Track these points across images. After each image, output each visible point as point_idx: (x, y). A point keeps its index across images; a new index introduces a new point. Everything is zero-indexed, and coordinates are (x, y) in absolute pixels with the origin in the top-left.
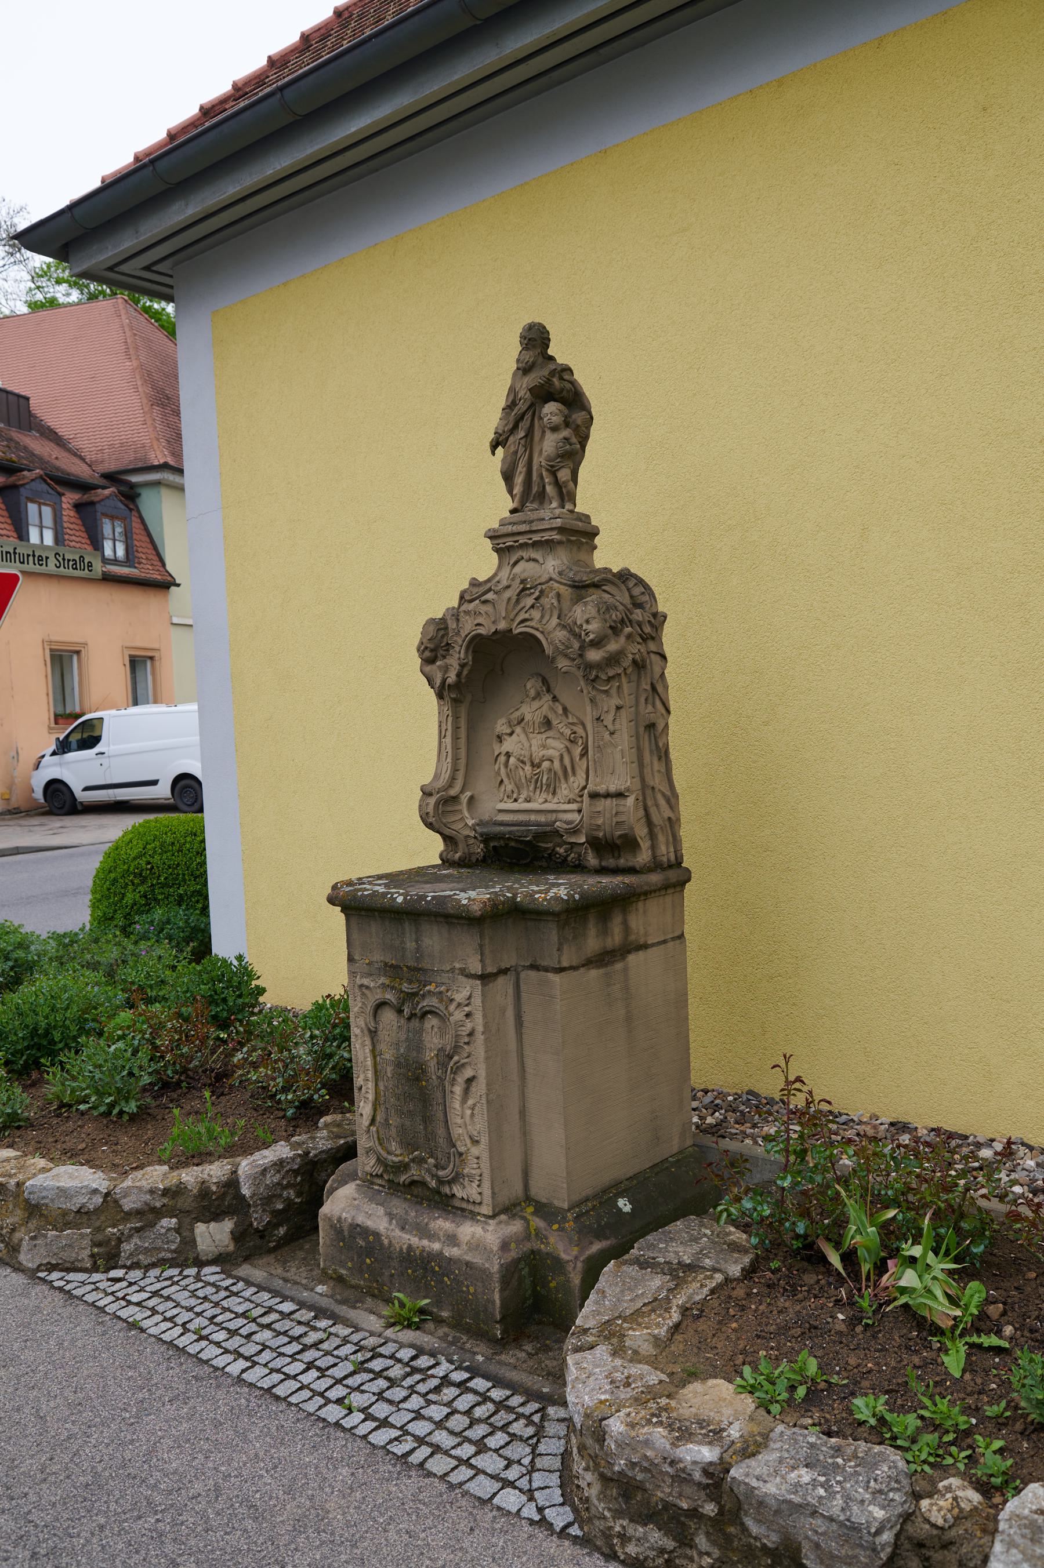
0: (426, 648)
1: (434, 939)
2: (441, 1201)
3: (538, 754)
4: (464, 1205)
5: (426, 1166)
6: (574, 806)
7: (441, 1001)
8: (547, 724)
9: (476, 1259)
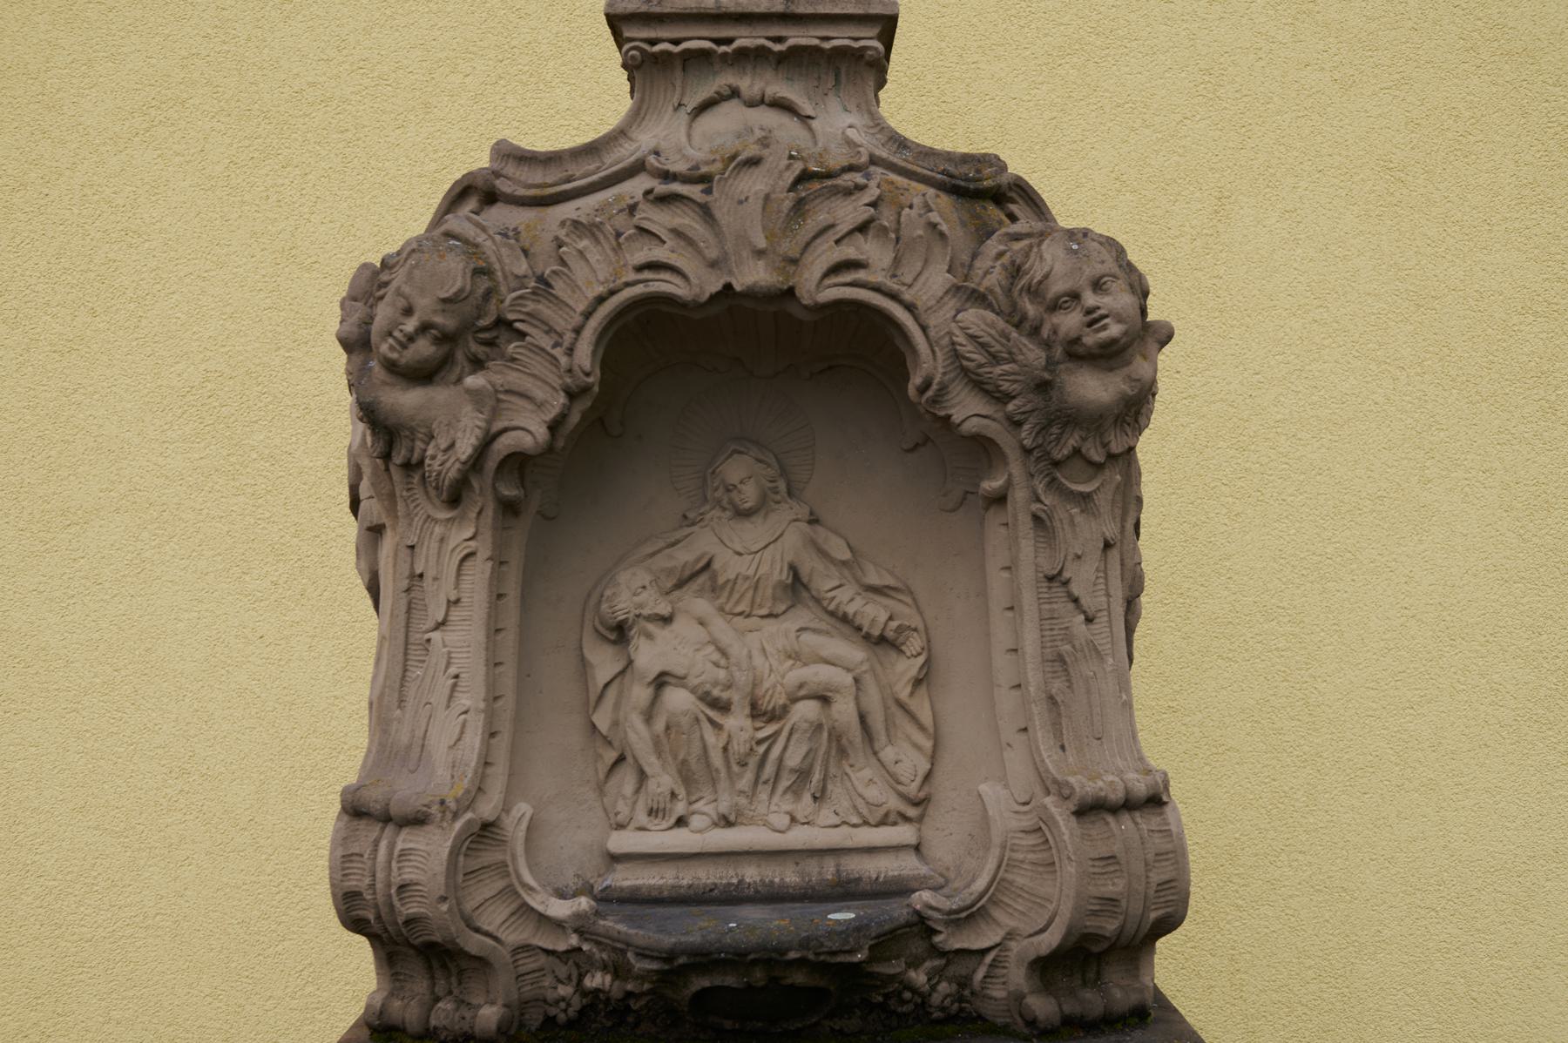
0: (424, 328)
3: (780, 678)
6: (903, 834)
8: (796, 586)
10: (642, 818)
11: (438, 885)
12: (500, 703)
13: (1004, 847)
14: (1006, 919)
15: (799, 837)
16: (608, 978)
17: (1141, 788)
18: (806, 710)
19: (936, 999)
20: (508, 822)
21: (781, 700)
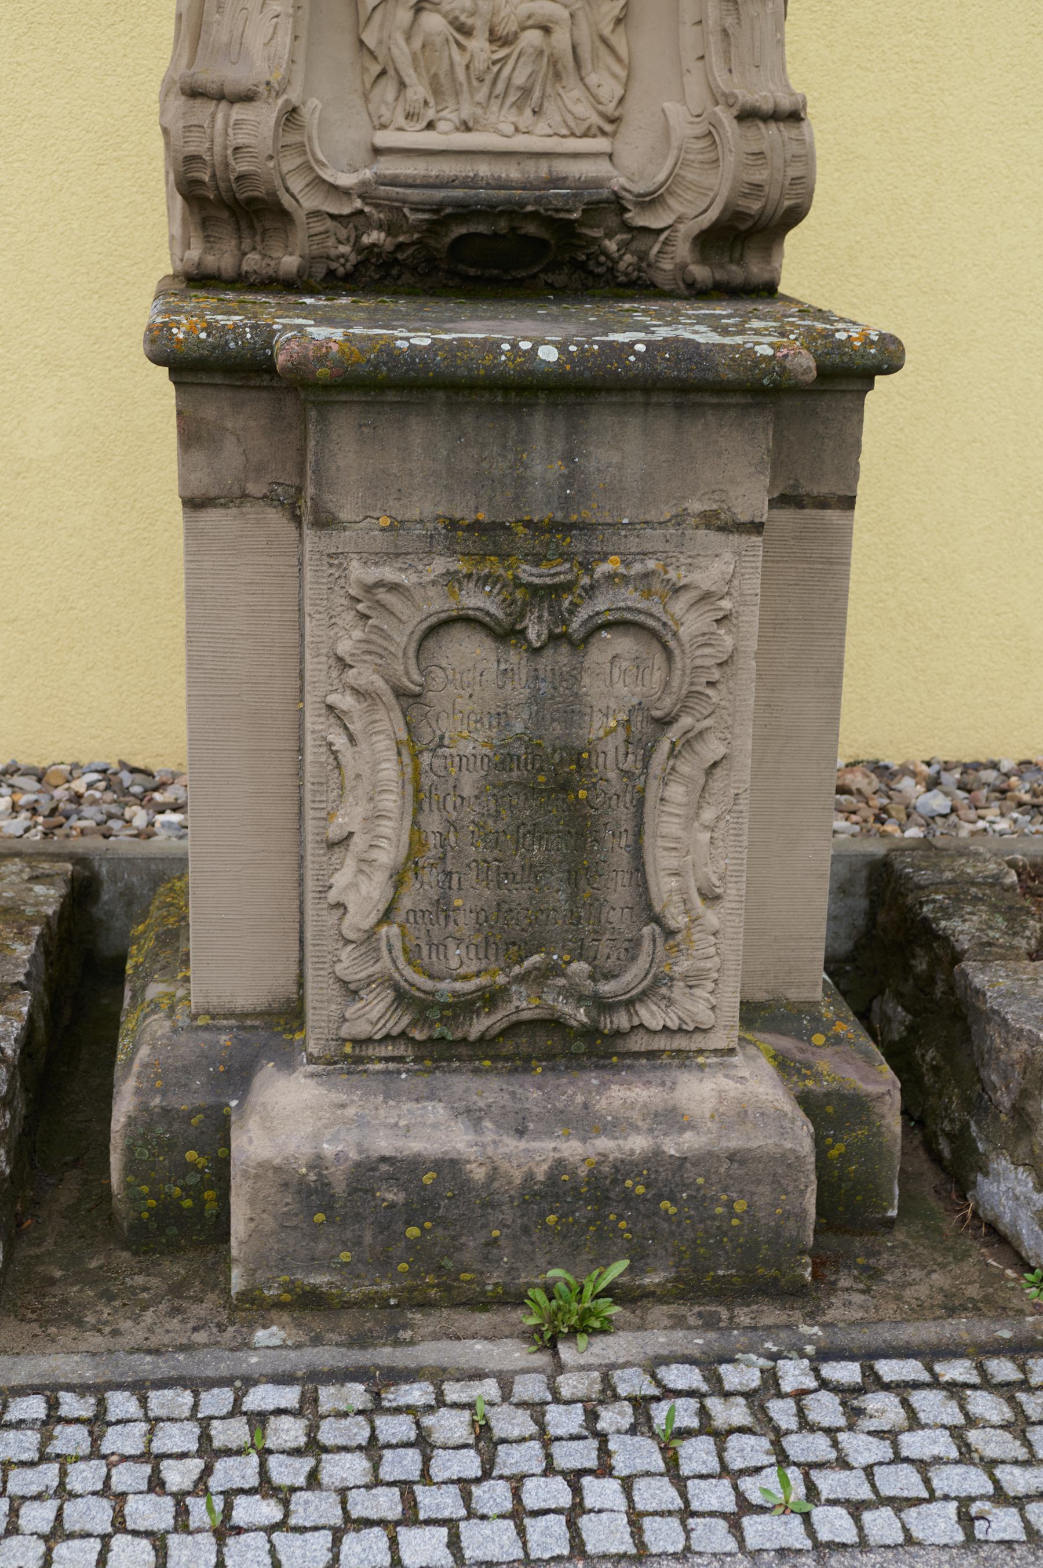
1: (622, 452)
2: (594, 1046)
4: (660, 1043)
5: (562, 982)
6: (601, 144)
7: (648, 594)
9: (759, 1140)
10: (401, 121)
11: (267, 147)
12: (300, 13)
13: (680, 149)
14: (677, 206)
15: (520, 143)
16: (383, 235)
17: (786, 104)
18: (532, 37)
19: (622, 266)
20: (305, 111)
21: (514, 27)
